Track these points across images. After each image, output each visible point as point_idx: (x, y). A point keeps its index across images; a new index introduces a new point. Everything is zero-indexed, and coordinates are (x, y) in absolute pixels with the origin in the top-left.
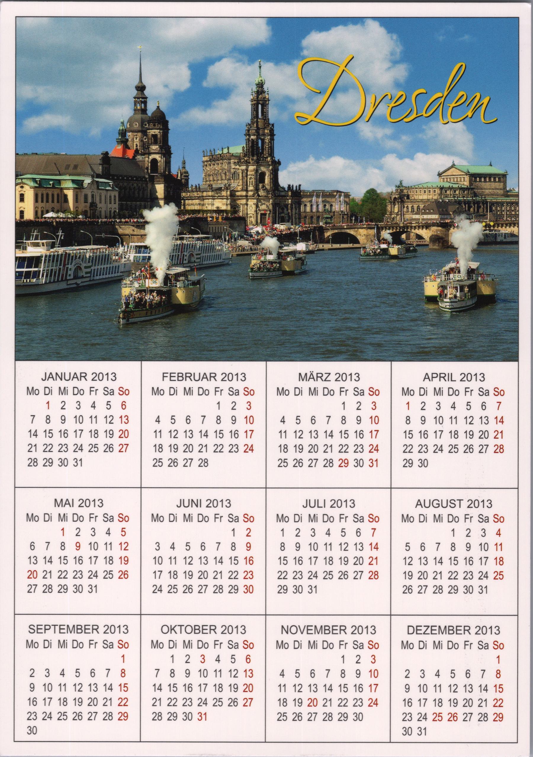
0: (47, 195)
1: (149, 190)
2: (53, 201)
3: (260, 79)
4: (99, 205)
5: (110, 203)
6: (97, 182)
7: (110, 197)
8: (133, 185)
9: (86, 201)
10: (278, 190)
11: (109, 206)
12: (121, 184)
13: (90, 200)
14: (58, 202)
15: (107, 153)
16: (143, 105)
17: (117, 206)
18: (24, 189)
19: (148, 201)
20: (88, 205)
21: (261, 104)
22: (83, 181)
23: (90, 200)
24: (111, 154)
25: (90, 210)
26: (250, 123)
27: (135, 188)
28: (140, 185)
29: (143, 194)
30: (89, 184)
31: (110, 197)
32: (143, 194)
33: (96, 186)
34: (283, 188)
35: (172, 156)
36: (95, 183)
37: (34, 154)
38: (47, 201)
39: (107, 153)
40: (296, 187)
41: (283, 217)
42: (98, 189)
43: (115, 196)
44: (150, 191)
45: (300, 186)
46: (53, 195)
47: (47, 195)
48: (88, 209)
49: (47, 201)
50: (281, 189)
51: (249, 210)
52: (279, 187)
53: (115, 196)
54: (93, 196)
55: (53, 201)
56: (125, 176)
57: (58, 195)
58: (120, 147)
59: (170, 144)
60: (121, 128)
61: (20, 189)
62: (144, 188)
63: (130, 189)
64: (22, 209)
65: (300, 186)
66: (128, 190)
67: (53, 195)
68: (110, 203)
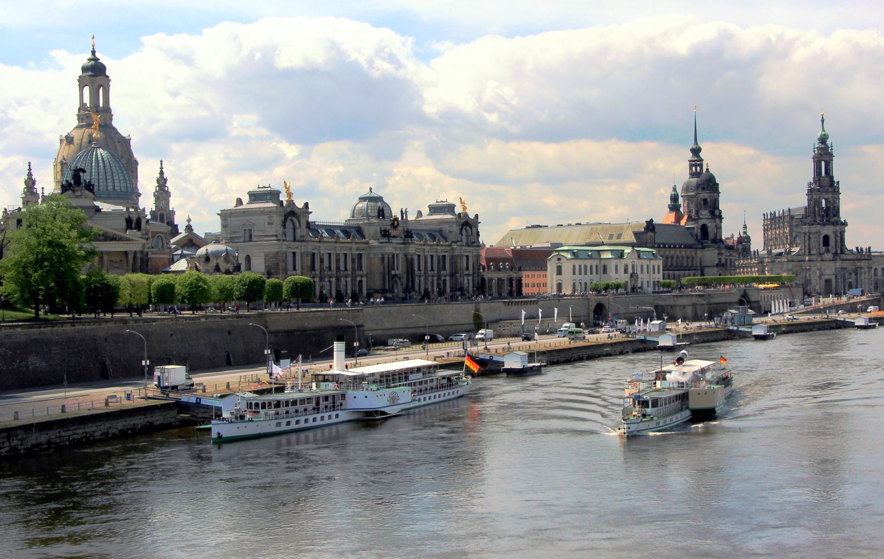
0: (586, 266)
1: (699, 257)
2: (591, 273)
3: (823, 133)
4: (640, 276)
5: (654, 272)
6: (638, 252)
7: (654, 266)
8: (680, 253)
9: (626, 271)
10: (844, 254)
11: (653, 276)
12: (667, 253)
13: (630, 271)
14: (597, 273)
15: (652, 220)
16: (698, 168)
17: (661, 275)
18: (561, 262)
19: (697, 270)
20: (628, 275)
21: (825, 161)
22: (624, 250)
23: (630, 271)
24: (657, 221)
25: (631, 281)
26: (812, 181)
27: (682, 256)
28: (688, 253)
29: (692, 263)
30: (629, 253)
31: (654, 266)
32: (692, 263)
33: (636, 255)
34: (851, 251)
35: (723, 220)
36: (635, 252)
37: (533, 227)
38: (586, 273)
39: (652, 220)
40: (866, 249)
41: (850, 282)
42: (639, 257)
43: (659, 266)
44: (700, 259)
45: (869, 248)
46: (591, 267)
47: (586, 266)
48: (628, 280)
49: (586, 273)
50: (848, 252)
51: (812, 276)
52: (846, 250)
53: (659, 266)
54: (633, 267)
55: (591, 273)
56: (672, 244)
57: (597, 266)
58: (673, 215)
59: (720, 208)
60: (673, 193)
61: (557, 262)
62: (692, 256)
63: (677, 257)
64: (560, 282)
65: (869, 248)
66: (675, 259)
67: (591, 267)
68: (654, 272)
